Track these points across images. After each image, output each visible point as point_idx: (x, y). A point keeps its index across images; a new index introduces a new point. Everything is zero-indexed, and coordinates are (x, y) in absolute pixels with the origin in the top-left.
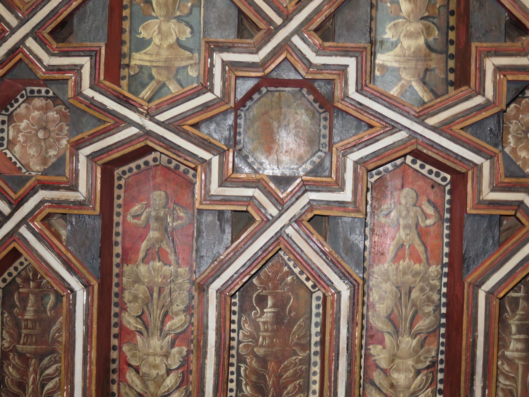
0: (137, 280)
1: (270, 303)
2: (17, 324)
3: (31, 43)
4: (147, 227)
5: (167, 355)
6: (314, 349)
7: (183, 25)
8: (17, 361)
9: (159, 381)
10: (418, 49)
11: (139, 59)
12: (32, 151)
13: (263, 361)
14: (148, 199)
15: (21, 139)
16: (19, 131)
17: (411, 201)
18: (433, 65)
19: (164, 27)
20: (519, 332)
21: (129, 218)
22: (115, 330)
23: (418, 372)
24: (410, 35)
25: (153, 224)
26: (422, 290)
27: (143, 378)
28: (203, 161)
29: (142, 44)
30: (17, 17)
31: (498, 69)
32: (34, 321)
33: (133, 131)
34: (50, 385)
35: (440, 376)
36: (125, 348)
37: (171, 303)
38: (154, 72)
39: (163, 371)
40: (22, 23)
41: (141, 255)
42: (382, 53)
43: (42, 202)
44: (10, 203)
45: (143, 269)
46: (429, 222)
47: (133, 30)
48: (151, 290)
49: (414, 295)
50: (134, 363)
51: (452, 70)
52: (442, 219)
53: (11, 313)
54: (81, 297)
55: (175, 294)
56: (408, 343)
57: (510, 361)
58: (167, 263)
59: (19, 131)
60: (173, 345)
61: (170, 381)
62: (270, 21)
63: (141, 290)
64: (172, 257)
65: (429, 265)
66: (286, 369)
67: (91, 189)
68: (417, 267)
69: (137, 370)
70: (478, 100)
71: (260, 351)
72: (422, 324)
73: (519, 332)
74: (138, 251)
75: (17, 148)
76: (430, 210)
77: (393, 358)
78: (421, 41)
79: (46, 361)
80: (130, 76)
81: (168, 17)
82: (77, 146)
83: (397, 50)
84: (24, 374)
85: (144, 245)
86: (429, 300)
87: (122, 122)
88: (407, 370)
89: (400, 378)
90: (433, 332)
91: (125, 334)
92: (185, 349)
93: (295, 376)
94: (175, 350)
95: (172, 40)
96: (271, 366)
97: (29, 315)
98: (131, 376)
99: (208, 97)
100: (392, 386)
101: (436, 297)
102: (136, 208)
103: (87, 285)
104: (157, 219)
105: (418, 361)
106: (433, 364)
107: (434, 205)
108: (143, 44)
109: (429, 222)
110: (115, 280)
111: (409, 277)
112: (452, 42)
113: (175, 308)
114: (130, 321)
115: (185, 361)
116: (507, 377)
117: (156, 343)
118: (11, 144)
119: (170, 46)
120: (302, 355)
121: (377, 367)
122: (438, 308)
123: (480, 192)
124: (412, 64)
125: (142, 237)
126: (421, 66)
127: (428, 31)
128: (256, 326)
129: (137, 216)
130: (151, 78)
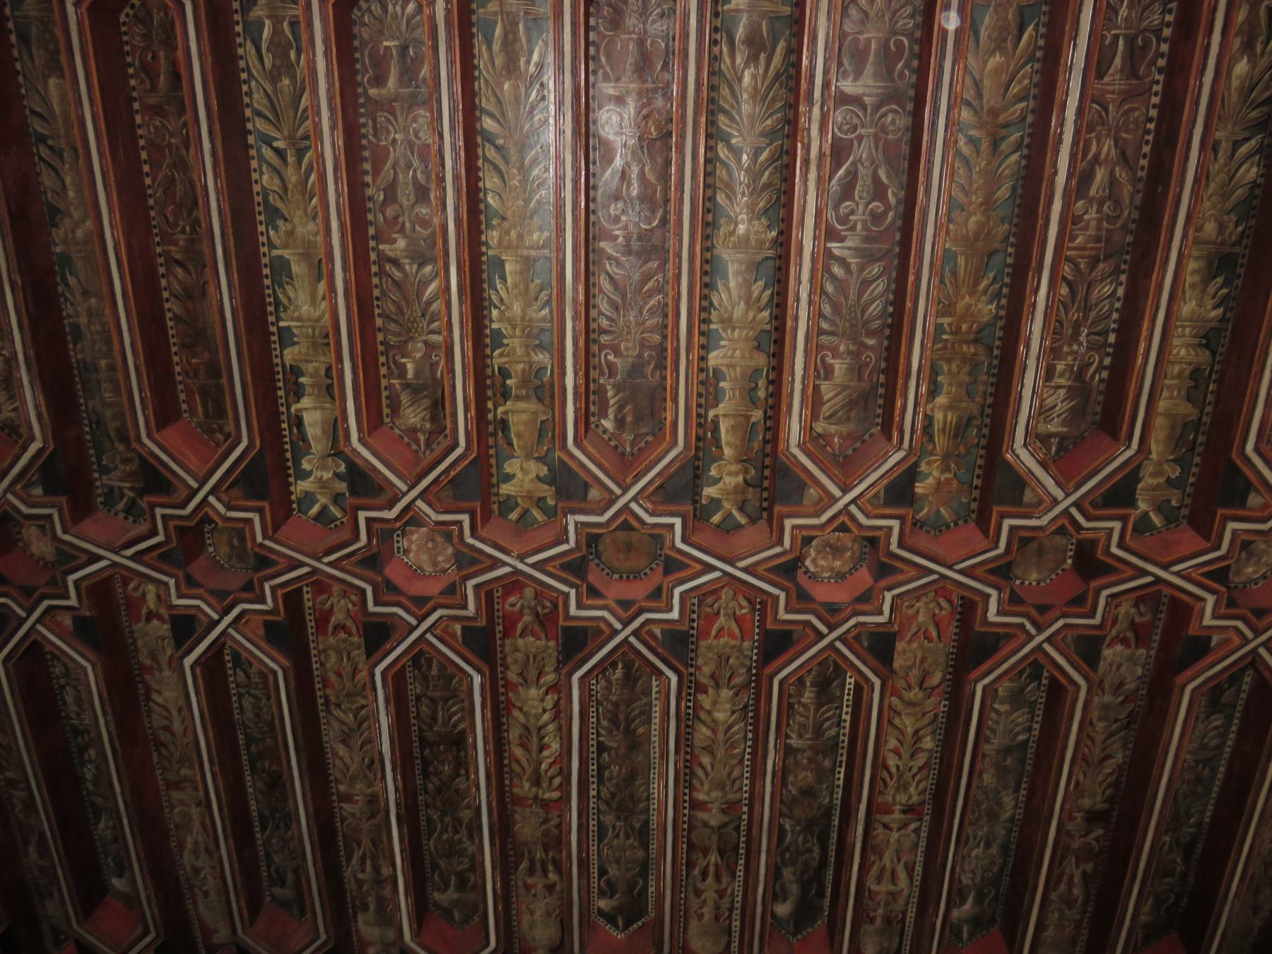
0: (517, 649)
1: (620, 666)
2: (426, 679)
3: (419, 503)
4: (521, 613)
5: (542, 700)
6: (654, 696)
7: (540, 465)
8: (427, 702)
9: (538, 717)
10: (737, 486)
11: (506, 489)
12: (424, 557)
13: (616, 705)
14: (521, 593)
15: (414, 547)
16: (412, 542)
17: (730, 597)
18: (750, 496)
19: (525, 465)
20: (812, 686)
21: (507, 606)
22: (501, 683)
23: (733, 712)
24: (730, 474)
25: (526, 611)
26: (738, 658)
27: (526, 715)
28: (563, 593)
29: (508, 478)
30: (406, 483)
31: (794, 527)
32: (439, 676)
33: (507, 569)
34: (455, 718)
35: (751, 714)
36: (510, 695)
37: (544, 666)
38: (519, 500)
39: (540, 710)
40: (411, 488)
41: (519, 632)
42: (709, 486)
43: (441, 618)
44: (416, 618)
45: (520, 642)
46: (743, 611)
47: (499, 466)
48: (528, 657)
49: (731, 661)
50: (518, 704)
51: (766, 500)
52: (754, 610)
53: (420, 670)
54: (477, 680)
55: (547, 660)
56: (726, 693)
57: (804, 706)
58: (538, 638)
59: (412, 542)
60: (547, 693)
61: (546, 717)
62: (612, 492)
63: (520, 656)
64: (543, 636)
65: (743, 639)
66: (634, 709)
67: (478, 609)
68: (733, 642)
69: (520, 709)
70: (778, 550)
71: (614, 698)
72: (737, 680)
73: (812, 686)
74: (515, 628)
75: (412, 555)
76: (744, 603)
77: (715, 703)
78: (741, 479)
79: (450, 702)
80: (500, 503)
81: (528, 457)
82: (466, 578)
83: (720, 485)
84: (435, 711)
85: (520, 626)
86: (743, 665)
87: (497, 563)
88: (726, 711)
89: (720, 716)
90: (746, 686)
91: (508, 685)
92: (556, 697)
93: (641, 714)
94: (549, 697)
95: (533, 475)
96: (622, 708)
97: (434, 672)
98: (516, 713)
99: (564, 547)
100: (714, 721)
101: (748, 663)
102: (512, 599)
103: (479, 671)
104: (529, 608)
105: (734, 705)
106: (746, 707)
107: (749, 601)
108: (508, 478)
109: (743, 611)
110: (499, 649)
111: (728, 650)
112: (766, 478)
113: (547, 669)
114: (513, 676)
115: (557, 704)
116: (801, 715)
117: (533, 692)
118: (406, 552)
119: (532, 480)
120: (645, 700)
121: (702, 708)
122: (749, 670)
123: (776, 613)
124: (733, 497)
125: (518, 621)
126: (740, 498)
127: (746, 472)
128: (608, 680)
129: (513, 605)
130: (517, 505)
